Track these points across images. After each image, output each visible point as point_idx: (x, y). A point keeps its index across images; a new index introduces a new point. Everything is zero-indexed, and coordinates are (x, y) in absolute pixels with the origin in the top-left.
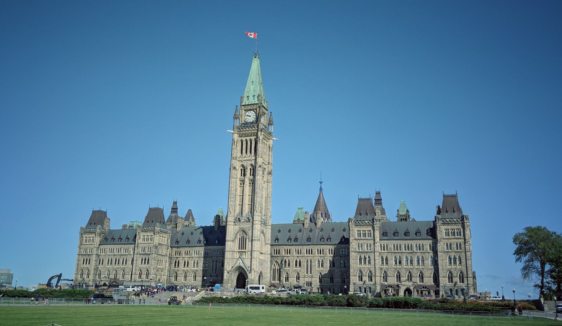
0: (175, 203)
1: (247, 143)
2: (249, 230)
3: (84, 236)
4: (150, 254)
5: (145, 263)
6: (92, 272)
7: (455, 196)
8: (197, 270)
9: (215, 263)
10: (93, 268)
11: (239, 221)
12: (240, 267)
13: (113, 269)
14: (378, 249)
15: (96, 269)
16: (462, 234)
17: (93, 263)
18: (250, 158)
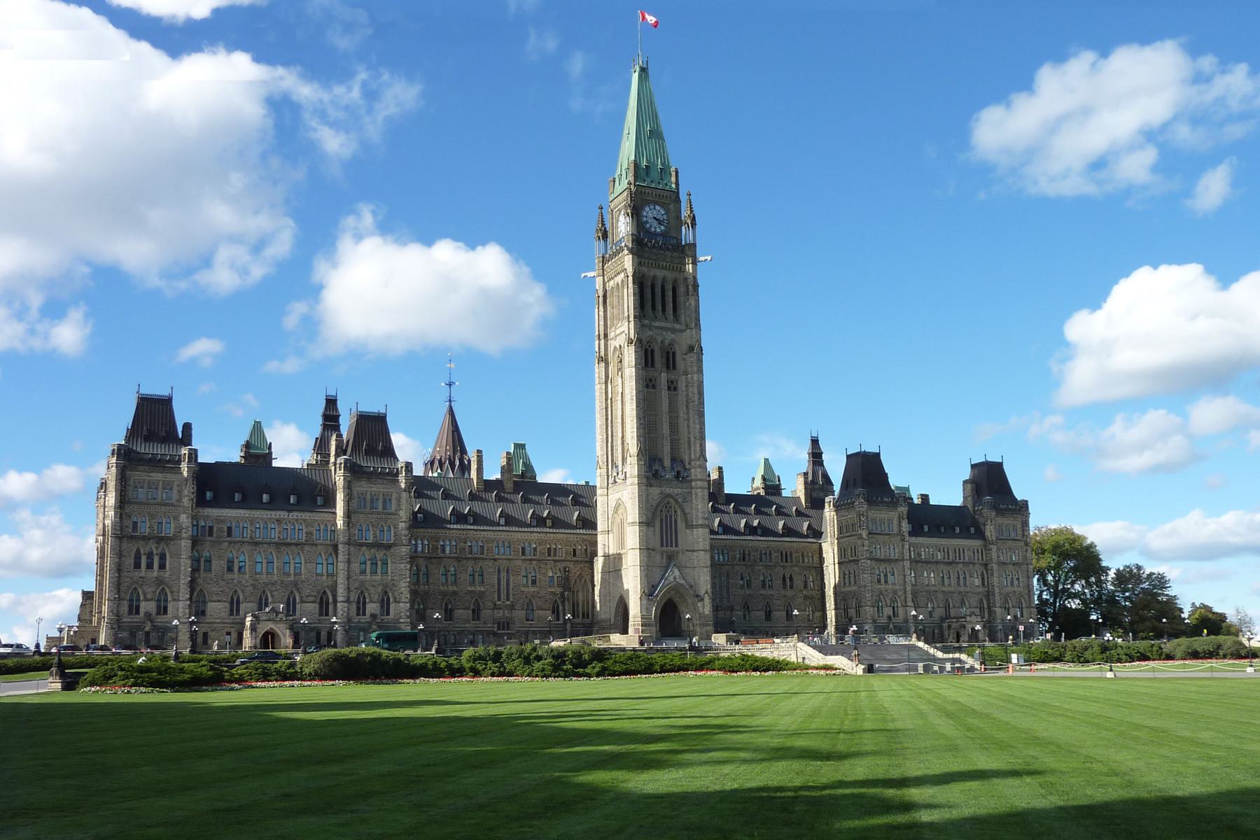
0: (331, 403)
1: (653, 286)
2: (685, 500)
3: (136, 475)
4: (389, 547)
5: (374, 572)
6: (184, 593)
7: (1000, 465)
8: (454, 593)
9: (503, 574)
10: (185, 580)
11: (656, 475)
12: (676, 588)
13: (254, 586)
14: (907, 556)
15: (192, 584)
16: (1020, 532)
17: (185, 565)
18: (669, 325)
